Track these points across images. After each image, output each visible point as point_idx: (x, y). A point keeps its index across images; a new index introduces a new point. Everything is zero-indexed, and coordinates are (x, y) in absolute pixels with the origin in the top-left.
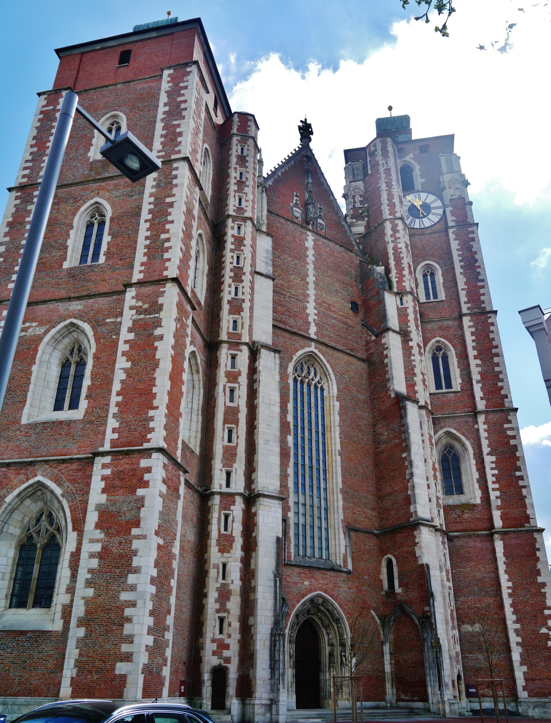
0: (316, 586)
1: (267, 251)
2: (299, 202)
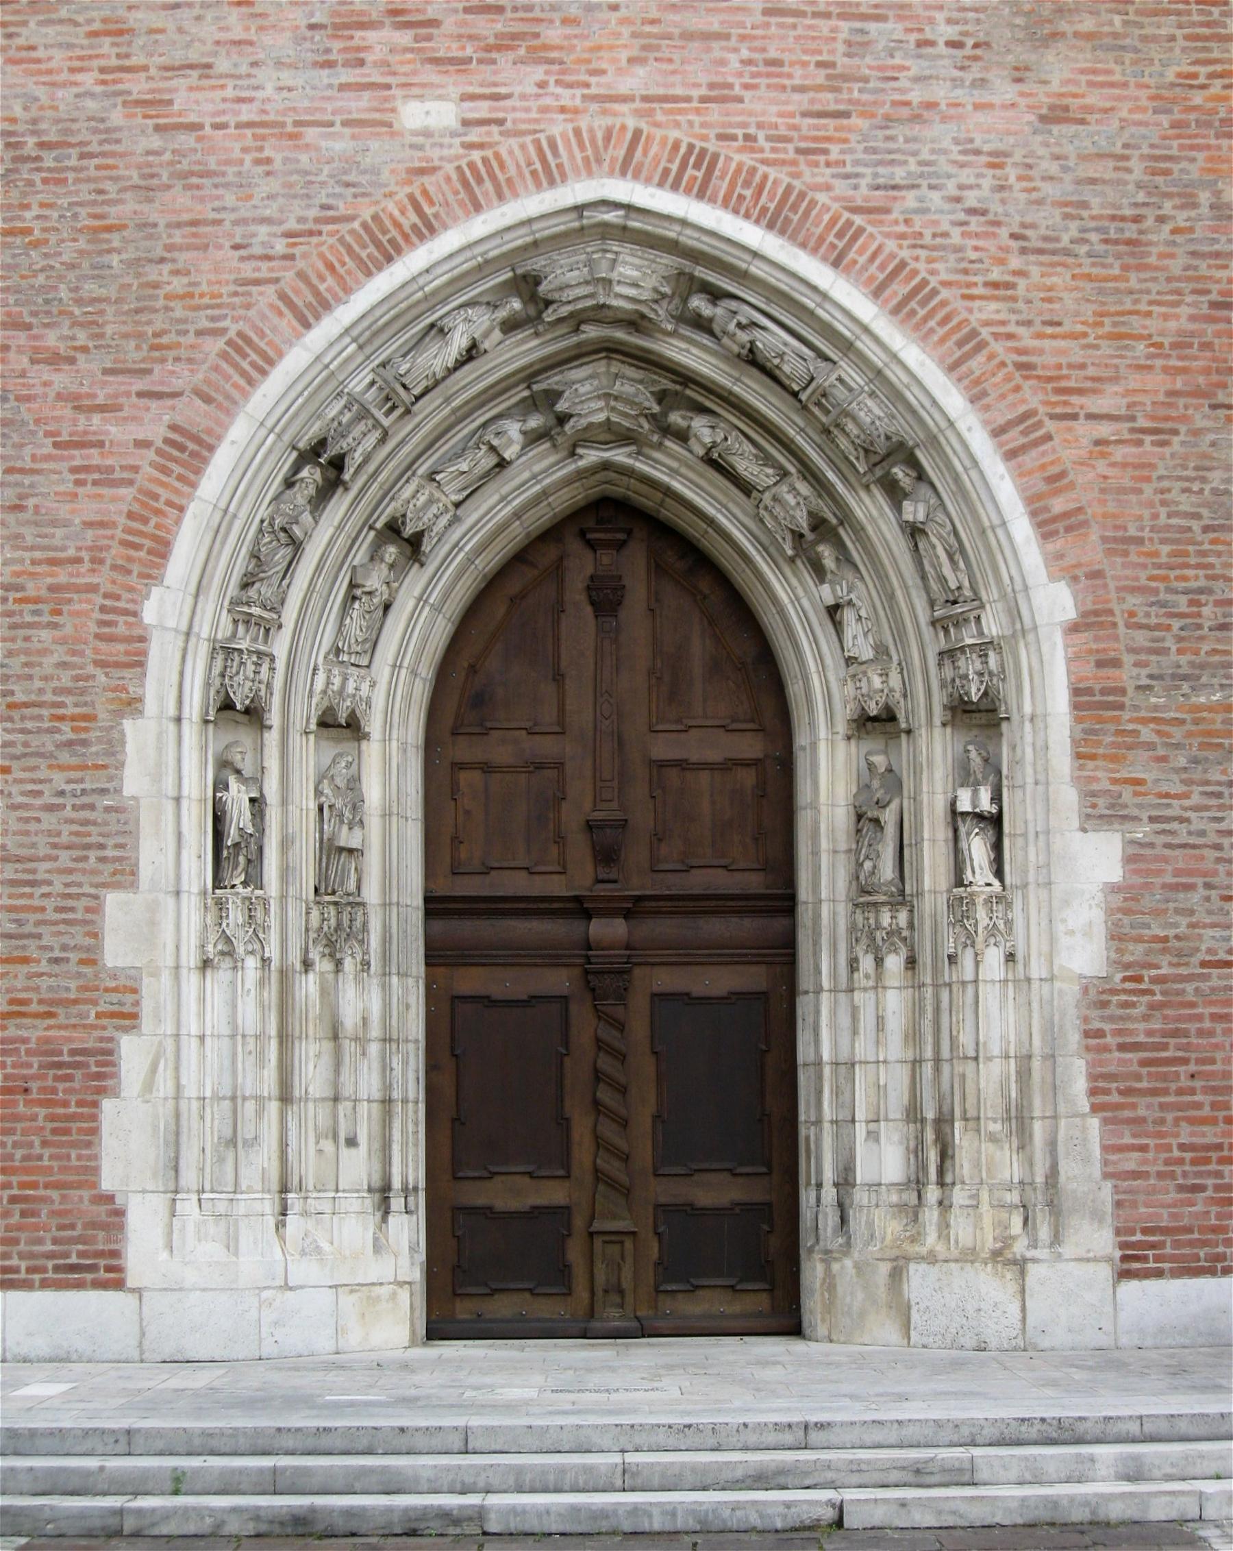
0: (558, 127)
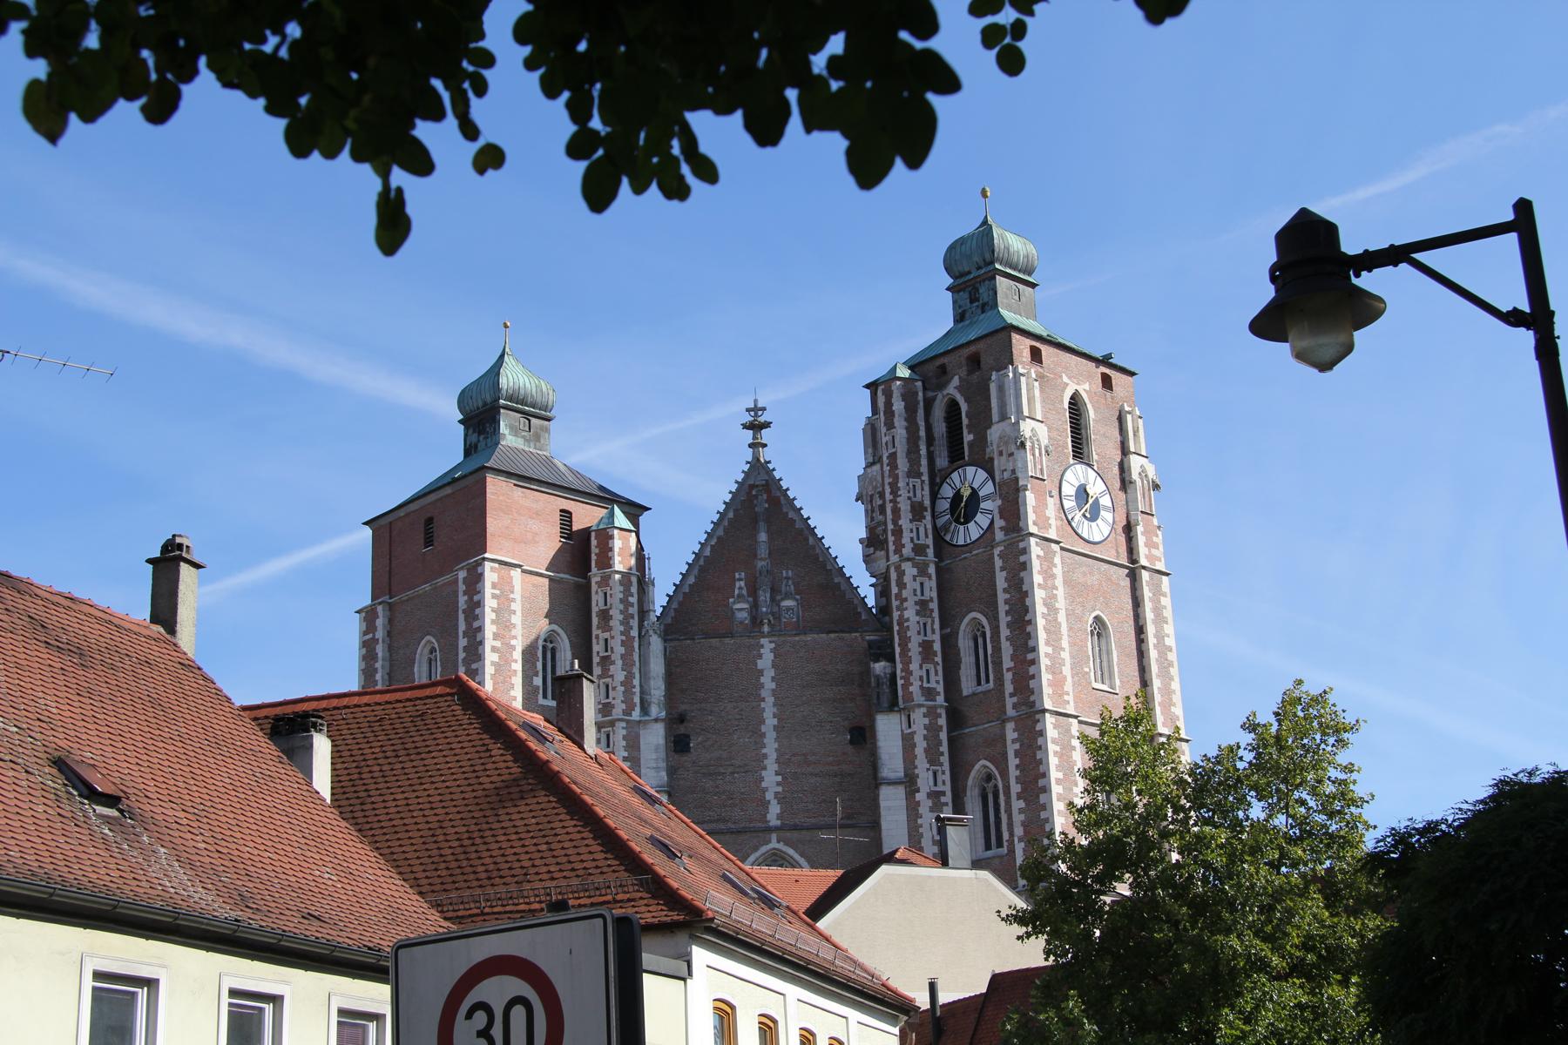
1: (657, 749)
2: (744, 592)
